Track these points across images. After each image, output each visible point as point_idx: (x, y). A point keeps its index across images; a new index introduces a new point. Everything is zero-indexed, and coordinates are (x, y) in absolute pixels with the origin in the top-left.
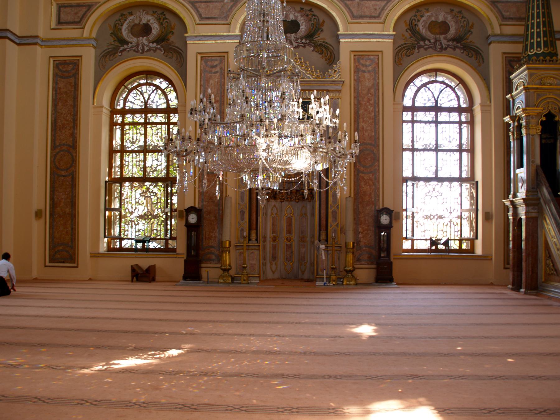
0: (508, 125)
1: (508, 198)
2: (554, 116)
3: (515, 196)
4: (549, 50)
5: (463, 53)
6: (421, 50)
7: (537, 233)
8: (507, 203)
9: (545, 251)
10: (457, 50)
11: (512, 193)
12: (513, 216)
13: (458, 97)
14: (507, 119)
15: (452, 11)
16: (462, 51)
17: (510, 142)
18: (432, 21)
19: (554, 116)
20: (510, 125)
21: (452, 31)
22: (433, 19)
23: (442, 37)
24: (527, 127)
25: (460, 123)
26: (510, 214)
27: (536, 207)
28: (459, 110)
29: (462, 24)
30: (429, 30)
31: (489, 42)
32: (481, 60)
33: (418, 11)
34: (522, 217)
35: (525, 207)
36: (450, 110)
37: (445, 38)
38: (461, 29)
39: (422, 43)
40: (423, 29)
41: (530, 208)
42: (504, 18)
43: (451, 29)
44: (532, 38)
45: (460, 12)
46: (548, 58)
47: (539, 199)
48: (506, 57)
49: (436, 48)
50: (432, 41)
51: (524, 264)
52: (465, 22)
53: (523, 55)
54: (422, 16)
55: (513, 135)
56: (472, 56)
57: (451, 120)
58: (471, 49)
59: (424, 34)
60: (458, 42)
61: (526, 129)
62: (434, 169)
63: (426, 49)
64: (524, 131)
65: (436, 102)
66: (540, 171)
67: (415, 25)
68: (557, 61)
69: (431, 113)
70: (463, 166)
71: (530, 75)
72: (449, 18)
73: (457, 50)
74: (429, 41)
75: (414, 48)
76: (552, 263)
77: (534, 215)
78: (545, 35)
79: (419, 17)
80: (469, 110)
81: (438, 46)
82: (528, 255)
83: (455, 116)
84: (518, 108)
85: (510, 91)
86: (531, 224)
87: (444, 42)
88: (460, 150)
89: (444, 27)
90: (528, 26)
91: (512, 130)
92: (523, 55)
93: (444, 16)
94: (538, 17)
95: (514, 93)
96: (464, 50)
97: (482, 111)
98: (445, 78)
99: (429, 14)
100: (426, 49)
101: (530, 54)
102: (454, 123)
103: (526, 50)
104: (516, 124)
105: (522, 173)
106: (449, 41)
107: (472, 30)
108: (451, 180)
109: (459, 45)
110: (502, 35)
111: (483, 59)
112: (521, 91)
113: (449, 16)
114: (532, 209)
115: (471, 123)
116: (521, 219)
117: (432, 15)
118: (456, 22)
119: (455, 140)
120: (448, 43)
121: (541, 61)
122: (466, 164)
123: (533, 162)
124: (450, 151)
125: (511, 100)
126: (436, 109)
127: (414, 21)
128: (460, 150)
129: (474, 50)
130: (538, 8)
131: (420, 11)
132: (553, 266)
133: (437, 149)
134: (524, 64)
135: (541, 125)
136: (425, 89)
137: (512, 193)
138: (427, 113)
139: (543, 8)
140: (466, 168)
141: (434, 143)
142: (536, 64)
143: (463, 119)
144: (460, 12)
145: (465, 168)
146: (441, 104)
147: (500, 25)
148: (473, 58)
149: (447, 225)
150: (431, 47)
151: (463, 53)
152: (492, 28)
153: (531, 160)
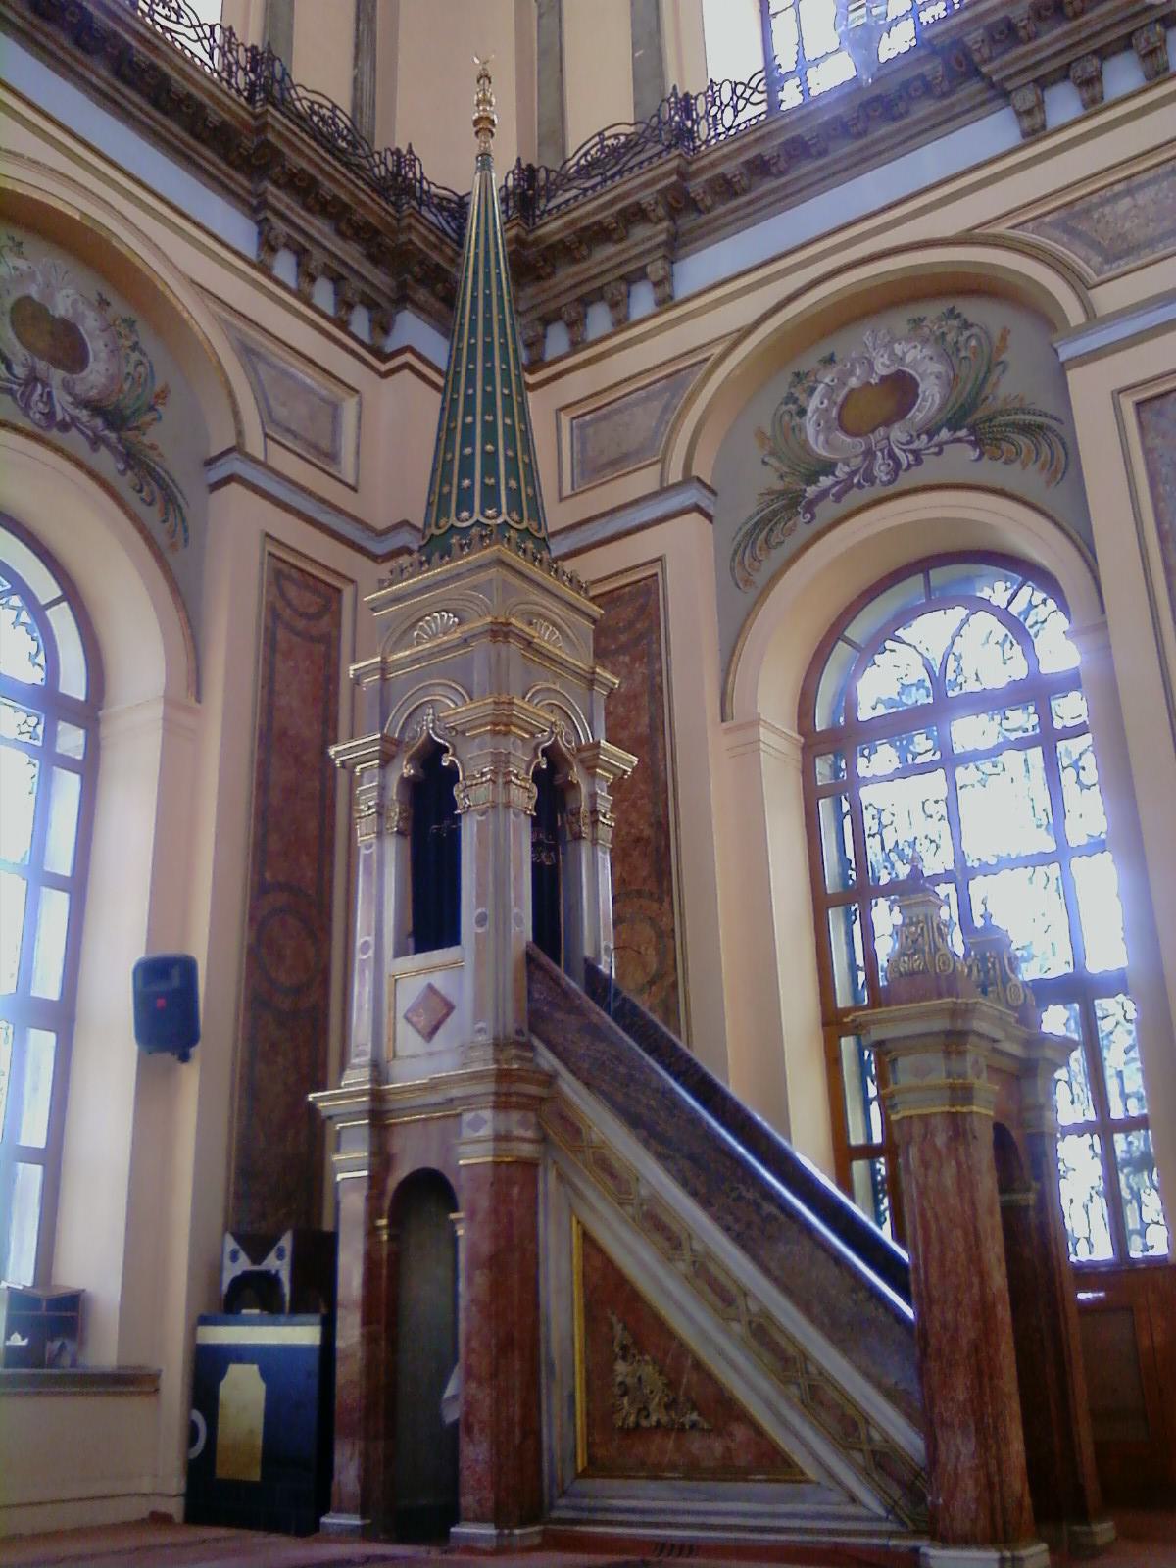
15: (103, 303)
16: (121, 466)
18: (29, 298)
21: (95, 375)
22: (34, 291)
23: (57, 376)
27: (532, 1117)
29: (130, 369)
30: (13, 323)
32: (180, 528)
37: (67, 387)
41: (515, 1116)
45: (130, 324)
47: (550, 1079)
48: (270, 554)
50: (20, 371)
52: (141, 369)
58: (151, 473)
60: (110, 425)
77: (527, 1150)
80: (90, 713)
87: (62, 401)
93: (74, 303)
96: (129, 467)
99: (22, 264)
107: (159, 407)
109: (112, 436)
110: (264, 465)
111: (186, 530)
115: (90, 769)
118: (114, 352)
120: (77, 412)
147: (266, 436)
150: (10, 392)
151: (123, 473)
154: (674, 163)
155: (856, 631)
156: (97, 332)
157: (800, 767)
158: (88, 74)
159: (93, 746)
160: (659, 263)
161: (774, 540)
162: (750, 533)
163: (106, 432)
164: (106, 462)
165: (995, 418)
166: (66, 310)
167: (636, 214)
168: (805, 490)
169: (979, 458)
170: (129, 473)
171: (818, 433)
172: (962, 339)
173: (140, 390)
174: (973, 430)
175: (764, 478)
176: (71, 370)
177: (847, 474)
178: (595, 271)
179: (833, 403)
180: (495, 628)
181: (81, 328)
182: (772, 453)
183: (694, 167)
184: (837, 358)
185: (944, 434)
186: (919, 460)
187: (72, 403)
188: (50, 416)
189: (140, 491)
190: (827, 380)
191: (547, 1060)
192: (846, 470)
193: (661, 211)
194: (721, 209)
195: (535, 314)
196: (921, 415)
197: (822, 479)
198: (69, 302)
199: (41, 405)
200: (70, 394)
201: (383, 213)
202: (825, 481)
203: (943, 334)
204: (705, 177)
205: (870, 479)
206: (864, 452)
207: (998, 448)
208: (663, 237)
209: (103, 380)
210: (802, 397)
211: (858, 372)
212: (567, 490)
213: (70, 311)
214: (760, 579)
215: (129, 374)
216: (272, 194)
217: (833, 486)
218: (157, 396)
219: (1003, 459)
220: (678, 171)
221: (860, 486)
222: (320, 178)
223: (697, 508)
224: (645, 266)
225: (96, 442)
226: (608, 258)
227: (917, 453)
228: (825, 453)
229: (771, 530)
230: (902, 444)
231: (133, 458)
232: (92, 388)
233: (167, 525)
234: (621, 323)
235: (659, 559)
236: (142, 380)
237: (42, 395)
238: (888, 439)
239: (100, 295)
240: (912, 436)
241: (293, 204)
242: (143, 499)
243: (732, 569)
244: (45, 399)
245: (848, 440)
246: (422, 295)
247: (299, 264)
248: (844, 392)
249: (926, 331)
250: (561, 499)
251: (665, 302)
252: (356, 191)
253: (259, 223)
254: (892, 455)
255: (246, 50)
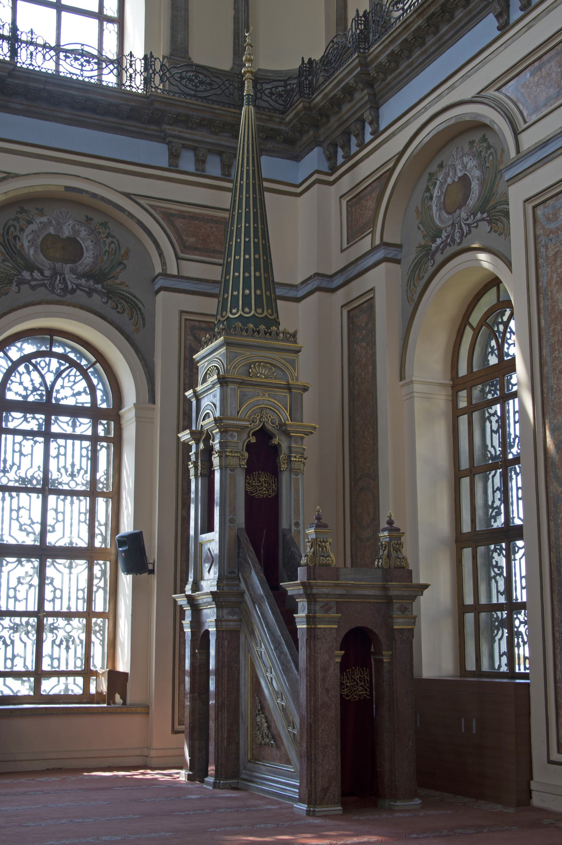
0: (187, 447)
1: (183, 591)
2: (271, 436)
3: (196, 587)
4: (265, 313)
5: (106, 303)
6: (25, 288)
7: (238, 662)
8: (182, 601)
9: (253, 697)
10: (95, 296)
11: (191, 580)
12: (192, 627)
13: (92, 389)
14: (185, 436)
15: (89, 219)
17: (189, 481)
19: (271, 436)
20: (191, 447)
21: (88, 258)
22: (51, 230)
24: (221, 454)
25: (94, 439)
26: (187, 622)
27: (237, 610)
28: (93, 413)
29: (107, 248)
31: (157, 287)
32: (140, 320)
33: (22, 211)
34: (210, 629)
35: (215, 610)
36: (75, 412)
37: (72, 271)
38: (105, 258)
39: (26, 275)
40: (29, 247)
41: (225, 611)
42: (185, 247)
43: (85, 254)
44: (236, 287)
45: (104, 225)
46: (262, 327)
47: (242, 594)
48: (186, 320)
49: (53, 288)
51: (212, 724)
52: (113, 246)
53: (219, 317)
54: (29, 222)
55: (196, 467)
56: (123, 313)
57: (78, 431)
59: (32, 257)
60: (97, 282)
61: (220, 457)
62: (37, 528)
63: (33, 288)
64: (216, 460)
65: (49, 393)
66: (245, 538)
67: (15, 237)
68: (277, 334)
69: (38, 416)
70: (97, 524)
71: (230, 358)
72: (83, 233)
73: (95, 296)
74: (42, 273)
75: (10, 282)
76: (267, 722)
77: (232, 625)
78: (258, 286)
79: (22, 222)
80: (114, 414)
81: (58, 285)
82: (219, 707)
83: (84, 426)
84: (207, 416)
85: (192, 384)
86: (226, 643)
87: (70, 278)
88: (92, 493)
89: (73, 249)
90: (229, 264)
91: (193, 458)
92: (219, 317)
94: (247, 251)
95: (199, 388)
96: (109, 298)
97: (139, 419)
98: (68, 350)
99: (44, 219)
100: (33, 288)
101: (231, 316)
102: (81, 438)
103: (224, 308)
104: (202, 446)
105: (212, 541)
106: (79, 277)
107: (125, 262)
108: (70, 553)
109: (99, 286)
111: (143, 319)
112: (214, 385)
113: (83, 228)
114: (230, 613)
116: (207, 632)
117: (50, 223)
119: (82, 472)
120: (79, 281)
121: (250, 331)
122: (103, 521)
123: (232, 521)
124: (73, 493)
125: (194, 401)
126: (48, 407)
127: (12, 229)
128: (92, 493)
129: (127, 300)
130: (247, 234)
131: (26, 212)
132: (269, 727)
133: (46, 488)
134: (220, 334)
135: (246, 450)
136: (27, 367)
137: (191, 580)
138: (28, 416)
139: (256, 236)
140: (103, 528)
141: (40, 475)
142: (242, 336)
143: (101, 432)
144: (104, 225)
145: (100, 529)
146: (57, 400)
147: (178, 258)
148: (126, 315)
149: (59, 646)
150: (44, 285)
151: (106, 303)
152: (164, 264)
153: (228, 518)
154: (357, 61)
155: (475, 318)
156: (87, 237)
157: (450, 398)
158: (60, 114)
159: (119, 430)
160: (368, 113)
161: (421, 276)
162: (413, 271)
163: (96, 286)
164: (97, 300)
165: (496, 206)
166: (69, 232)
167: (349, 91)
168: (431, 246)
169: (490, 232)
170: (110, 301)
171: (437, 210)
172: (487, 155)
173: (113, 256)
174: (488, 212)
175: (419, 239)
176: (74, 261)
177: (446, 237)
178: (345, 117)
179: (442, 192)
180: (221, 380)
181: (78, 239)
182: (421, 222)
183: (369, 59)
184: (444, 165)
185: (479, 216)
186: (470, 232)
187: (76, 278)
188: (65, 289)
189: (117, 307)
190: (440, 179)
191: (243, 585)
192: (446, 234)
193: (361, 85)
194: (389, 78)
195: (328, 142)
196: (471, 202)
197: (437, 239)
198: (70, 228)
199: (60, 285)
200: (74, 274)
201: (233, 114)
202: (439, 241)
203: (481, 152)
204: (375, 64)
205: (453, 241)
206: (452, 224)
207: (497, 225)
208: (367, 98)
209: (92, 260)
210: (432, 188)
211: (451, 174)
212: (345, 246)
213: (72, 232)
214: (416, 297)
215: (106, 251)
216: (169, 129)
217: (441, 244)
218: (123, 256)
219: (498, 232)
220: (360, 64)
221: (450, 246)
222: (190, 113)
223: (386, 260)
224: (363, 114)
225: (90, 294)
226: (349, 110)
227: (469, 225)
228: (440, 225)
229: (420, 269)
230: (465, 220)
231: (110, 294)
232: (86, 266)
233: (133, 320)
234: (362, 145)
235: (372, 289)
236: (113, 251)
237: (60, 281)
238: (460, 216)
239: (87, 217)
240: (468, 215)
241: (181, 129)
242: (118, 312)
243: (407, 291)
244: (62, 281)
245: (447, 216)
246: (270, 145)
247: (195, 155)
248: (445, 186)
249: (475, 149)
250: (342, 251)
251: (376, 133)
252: (214, 111)
253: (167, 144)
254: (461, 228)
255: (140, 60)
